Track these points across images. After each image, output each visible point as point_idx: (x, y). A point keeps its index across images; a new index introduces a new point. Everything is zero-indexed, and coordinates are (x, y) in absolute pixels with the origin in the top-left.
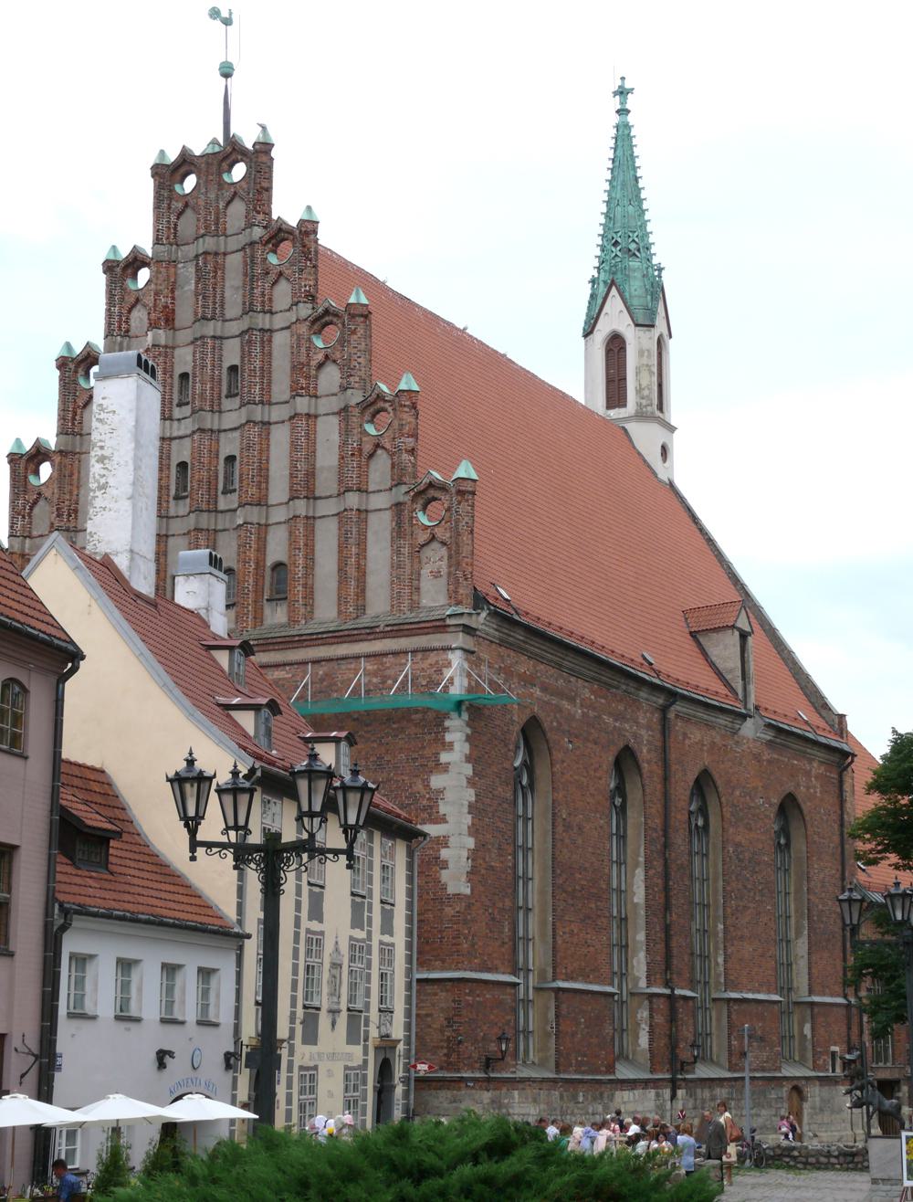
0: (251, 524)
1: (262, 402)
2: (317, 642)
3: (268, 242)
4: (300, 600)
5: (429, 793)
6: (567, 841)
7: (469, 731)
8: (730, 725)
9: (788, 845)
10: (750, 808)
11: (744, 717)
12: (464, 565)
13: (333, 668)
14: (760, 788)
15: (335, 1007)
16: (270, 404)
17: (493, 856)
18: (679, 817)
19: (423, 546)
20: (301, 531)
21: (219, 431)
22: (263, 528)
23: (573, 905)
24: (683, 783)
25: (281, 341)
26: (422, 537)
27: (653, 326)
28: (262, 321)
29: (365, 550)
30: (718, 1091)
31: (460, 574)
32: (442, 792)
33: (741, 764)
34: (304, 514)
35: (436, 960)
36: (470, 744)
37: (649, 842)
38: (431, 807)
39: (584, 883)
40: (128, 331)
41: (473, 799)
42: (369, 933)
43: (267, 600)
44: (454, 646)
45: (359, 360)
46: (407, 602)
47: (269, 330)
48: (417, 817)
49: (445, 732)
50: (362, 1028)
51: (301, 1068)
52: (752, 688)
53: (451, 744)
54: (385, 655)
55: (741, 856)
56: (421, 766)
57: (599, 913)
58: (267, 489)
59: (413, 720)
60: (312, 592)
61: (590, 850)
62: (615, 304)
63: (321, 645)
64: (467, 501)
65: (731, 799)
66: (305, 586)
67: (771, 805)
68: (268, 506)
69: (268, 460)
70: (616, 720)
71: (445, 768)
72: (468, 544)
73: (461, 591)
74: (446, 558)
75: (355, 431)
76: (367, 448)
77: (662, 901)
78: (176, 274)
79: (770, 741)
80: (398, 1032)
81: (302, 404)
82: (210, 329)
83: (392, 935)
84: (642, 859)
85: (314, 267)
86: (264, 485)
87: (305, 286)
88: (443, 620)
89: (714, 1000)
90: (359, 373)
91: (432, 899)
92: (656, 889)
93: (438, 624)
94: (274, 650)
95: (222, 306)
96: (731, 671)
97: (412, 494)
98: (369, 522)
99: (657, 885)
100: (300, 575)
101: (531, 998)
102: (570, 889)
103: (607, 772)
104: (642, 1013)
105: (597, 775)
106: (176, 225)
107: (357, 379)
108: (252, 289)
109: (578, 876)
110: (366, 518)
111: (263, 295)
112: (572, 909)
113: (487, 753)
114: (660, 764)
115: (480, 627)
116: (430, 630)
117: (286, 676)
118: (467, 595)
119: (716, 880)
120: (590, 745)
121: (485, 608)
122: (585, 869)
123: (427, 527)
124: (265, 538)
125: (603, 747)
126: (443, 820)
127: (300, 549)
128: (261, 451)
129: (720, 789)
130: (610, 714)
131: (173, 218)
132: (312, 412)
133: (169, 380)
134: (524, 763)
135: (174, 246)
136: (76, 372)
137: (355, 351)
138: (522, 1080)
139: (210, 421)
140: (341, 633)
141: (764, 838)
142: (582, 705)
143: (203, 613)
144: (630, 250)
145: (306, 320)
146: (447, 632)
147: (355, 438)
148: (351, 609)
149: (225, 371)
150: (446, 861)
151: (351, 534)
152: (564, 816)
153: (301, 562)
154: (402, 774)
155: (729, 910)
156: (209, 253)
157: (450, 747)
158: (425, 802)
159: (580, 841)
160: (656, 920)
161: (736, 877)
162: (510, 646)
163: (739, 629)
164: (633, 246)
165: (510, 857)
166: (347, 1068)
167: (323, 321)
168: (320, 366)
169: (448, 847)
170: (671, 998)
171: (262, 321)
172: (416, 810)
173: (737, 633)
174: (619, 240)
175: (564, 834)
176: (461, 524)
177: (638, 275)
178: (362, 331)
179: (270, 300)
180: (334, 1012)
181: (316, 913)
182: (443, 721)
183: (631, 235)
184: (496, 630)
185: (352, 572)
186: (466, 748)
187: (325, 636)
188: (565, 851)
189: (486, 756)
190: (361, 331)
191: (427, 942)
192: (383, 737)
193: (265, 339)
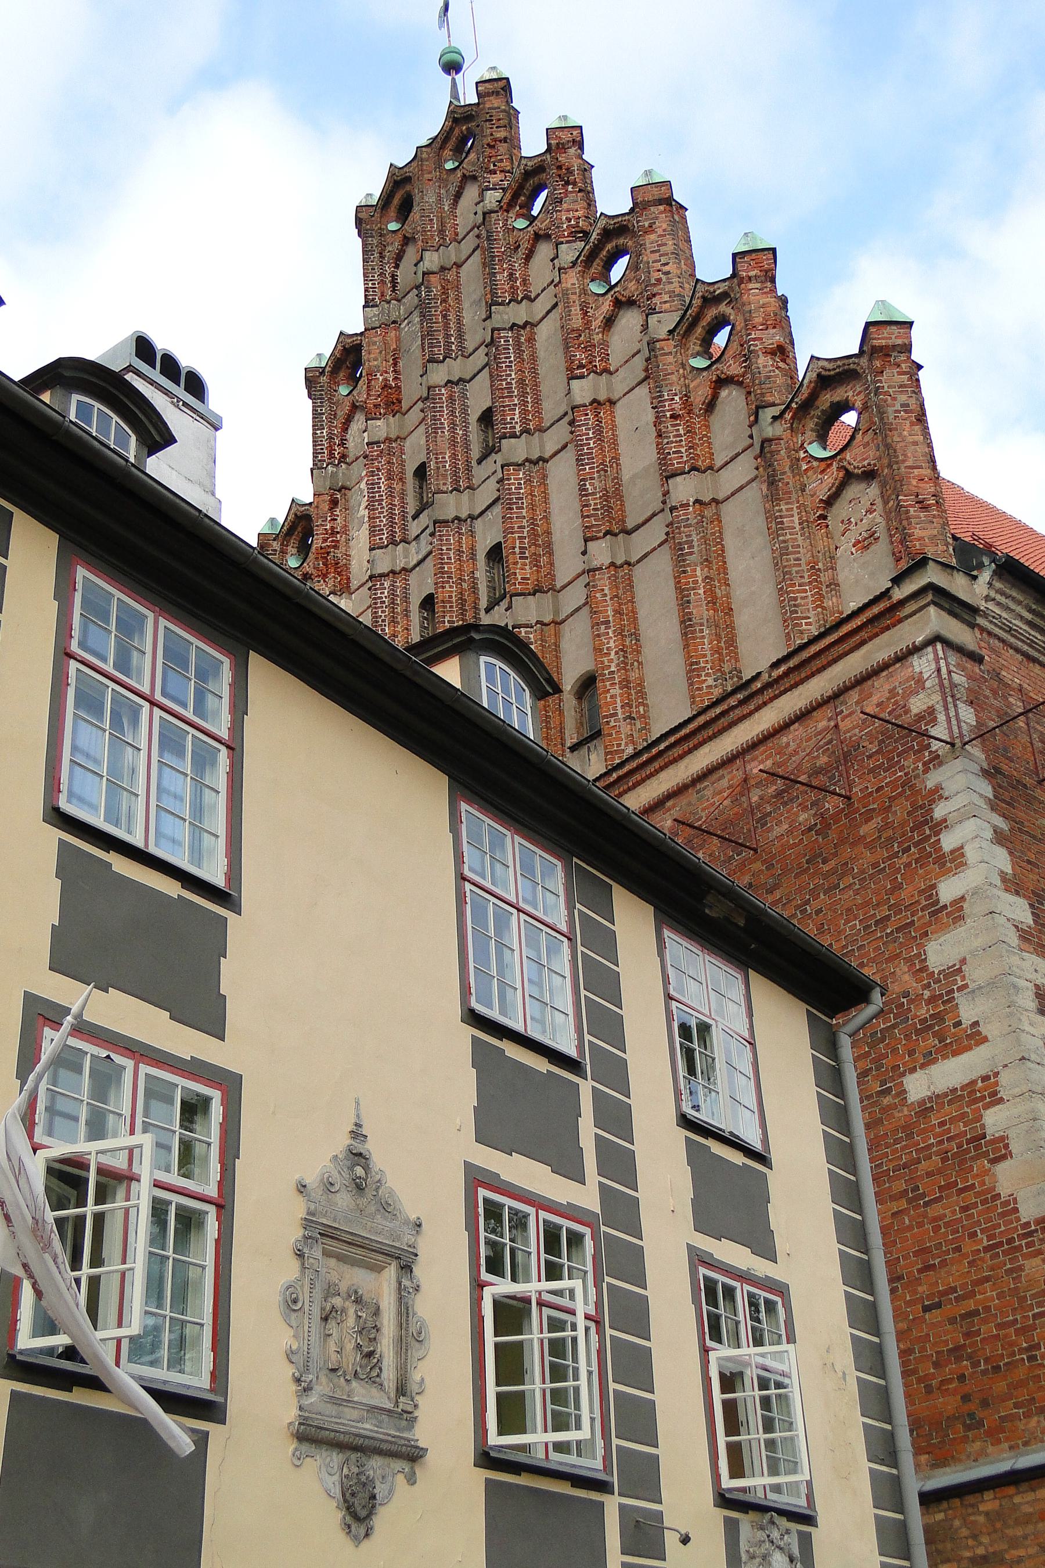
0: (526, 626)
1: (526, 431)
2: (649, 769)
4: (620, 712)
5: (928, 985)
12: (914, 482)
13: (689, 804)
16: (542, 430)
19: (829, 502)
20: (606, 591)
21: (473, 518)
25: (547, 333)
26: (821, 485)
28: (519, 313)
29: (724, 569)
32: (960, 970)
34: (607, 562)
35: (1028, 1415)
36: (1011, 853)
38: (939, 1017)
40: (343, 457)
44: (919, 640)
45: (666, 268)
46: (812, 614)
47: (527, 323)
48: (911, 1053)
49: (937, 834)
53: (958, 853)
56: (898, 930)
58: (552, 564)
59: (864, 837)
60: (642, 694)
63: (661, 769)
66: (625, 684)
69: (546, 518)
71: (956, 912)
72: (916, 443)
73: (918, 533)
74: (879, 501)
76: (701, 393)
78: (398, 339)
81: (583, 390)
85: (580, 191)
86: (544, 560)
87: (569, 220)
88: (885, 594)
91: (987, 1249)
93: (876, 610)
97: (788, 416)
106: (394, 277)
107: (666, 298)
115: (983, 605)
116: (864, 634)
121: (986, 561)
124: (557, 645)
126: (975, 1037)
128: (532, 507)
131: (388, 269)
132: (602, 397)
137: (656, 256)
139: (450, 505)
140: (692, 726)
145: (574, 264)
146: (900, 621)
147: (676, 388)
148: (710, 681)
149: (473, 426)
150: (1002, 1139)
151: (691, 547)
153: (612, 644)
157: (957, 860)
158: (924, 1011)
168: (609, 322)
169: (1001, 1100)
171: (519, 313)
172: (907, 1037)
176: (890, 410)
178: (664, 226)
179: (525, 282)
182: (931, 810)
184: (1030, 623)
185: (700, 611)
186: (1002, 860)
187: (662, 747)
190: (662, 224)
191: (997, 1369)
192: (807, 902)
193: (523, 339)
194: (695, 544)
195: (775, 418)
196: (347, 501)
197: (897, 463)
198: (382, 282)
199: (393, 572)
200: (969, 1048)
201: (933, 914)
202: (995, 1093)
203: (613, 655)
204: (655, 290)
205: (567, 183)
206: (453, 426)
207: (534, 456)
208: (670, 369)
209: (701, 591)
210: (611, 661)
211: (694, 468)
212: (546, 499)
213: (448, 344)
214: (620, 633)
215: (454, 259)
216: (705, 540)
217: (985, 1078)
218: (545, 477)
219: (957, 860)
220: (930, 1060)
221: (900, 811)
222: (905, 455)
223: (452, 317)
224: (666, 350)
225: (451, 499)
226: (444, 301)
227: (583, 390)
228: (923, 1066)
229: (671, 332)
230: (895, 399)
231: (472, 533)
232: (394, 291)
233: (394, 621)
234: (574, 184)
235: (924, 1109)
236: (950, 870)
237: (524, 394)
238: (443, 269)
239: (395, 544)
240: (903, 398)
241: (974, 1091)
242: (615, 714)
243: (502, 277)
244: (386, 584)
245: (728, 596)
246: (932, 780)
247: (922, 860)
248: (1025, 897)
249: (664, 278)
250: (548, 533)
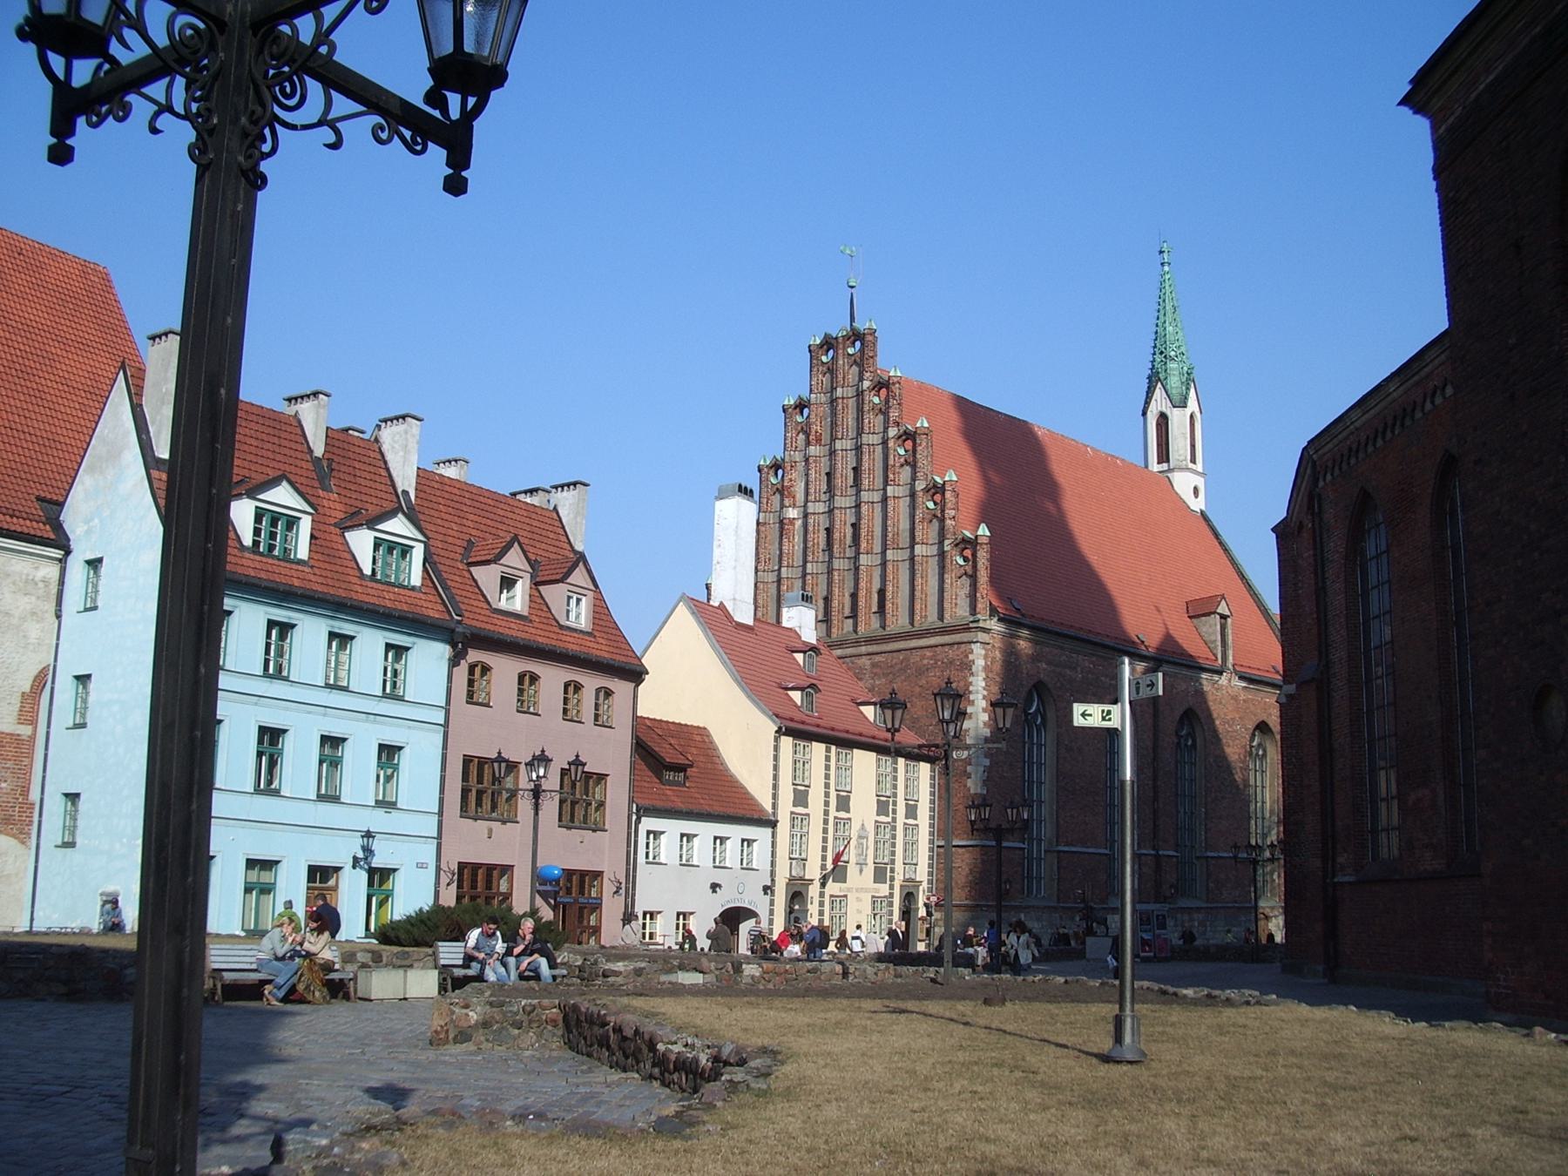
7: (985, 693)
9: (1265, 755)
11: (1220, 673)
15: (862, 862)
30: (1195, 916)
33: (1221, 703)
41: (989, 735)
42: (894, 820)
50: (888, 874)
51: (831, 896)
52: (1230, 653)
54: (936, 646)
62: (1159, 392)
80: (922, 874)
83: (916, 819)
89: (1198, 858)
111: (870, 423)
114: (1151, 706)
123: (961, 566)
129: (1203, 720)
130: (1107, 676)
134: (1038, 709)
138: (1029, 907)
142: (1082, 672)
143: (797, 629)
155: (1209, 799)
164: (1173, 353)
166: (873, 897)
170: (1157, 857)
173: (1218, 617)
177: (1176, 373)
180: (861, 865)
181: (844, 804)
219: (972, 703)
221: (962, 684)
246: (971, 679)
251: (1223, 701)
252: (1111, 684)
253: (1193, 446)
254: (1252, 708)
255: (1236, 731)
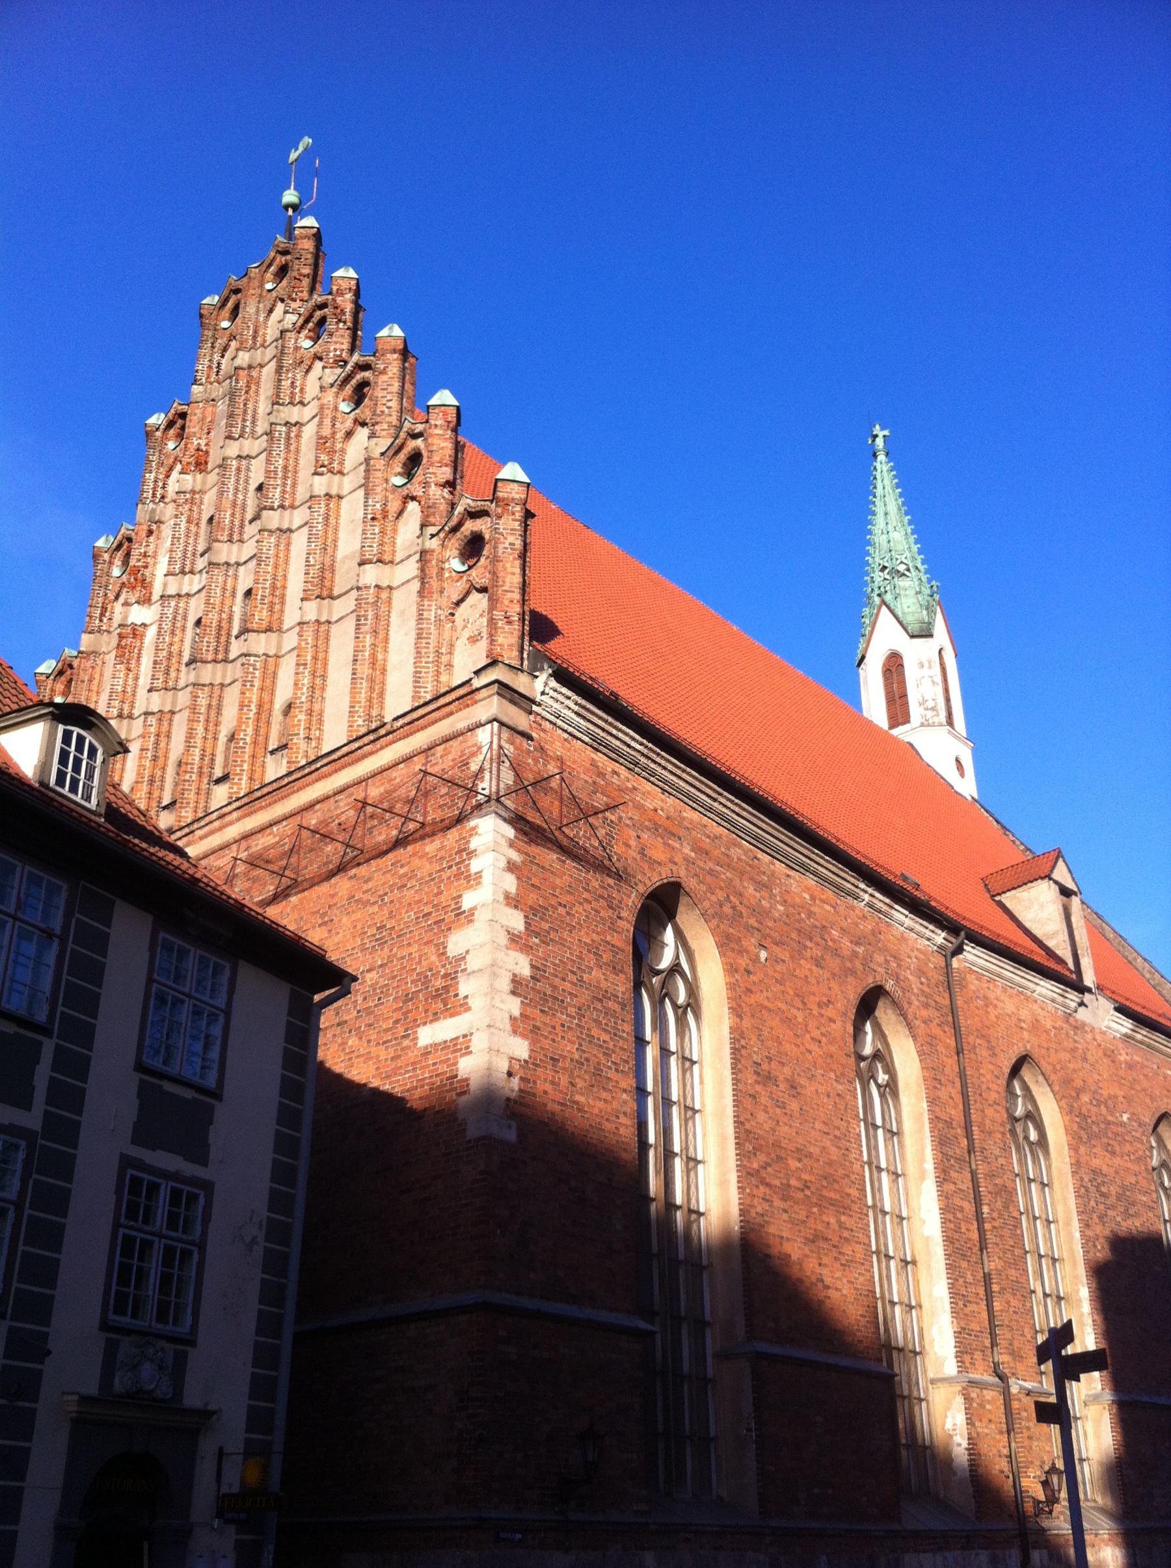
0: (256, 656)
1: (282, 507)
3: (302, 327)
4: (302, 732)
5: (444, 966)
6: (764, 1100)
8: (1060, 999)
10: (1109, 1123)
12: (506, 602)
13: (329, 810)
14: (1121, 1099)
17: (580, 1084)
18: (990, 1112)
21: (238, 564)
22: (271, 661)
23: (785, 1211)
24: (991, 1067)
25: (309, 431)
27: (931, 636)
28: (294, 414)
31: (499, 615)
32: (464, 958)
33: (1085, 1059)
34: (313, 620)
36: (518, 878)
37: (942, 1142)
38: (446, 989)
39: (806, 1177)
41: (526, 971)
43: (272, 753)
47: (297, 423)
48: (426, 1011)
49: (470, 859)
55: (1103, 1189)
56: (435, 923)
57: (846, 1234)
59: (428, 853)
61: (818, 1125)
63: (317, 781)
64: (513, 514)
65: (1075, 1105)
66: (310, 713)
67: (1140, 1125)
68: (280, 630)
69: (285, 576)
70: (857, 944)
75: (379, 489)
76: (393, 507)
77: (975, 1236)
79: (1126, 1035)
81: (320, 485)
82: (233, 449)
84: (929, 1166)
86: (277, 607)
87: (335, 350)
88: (469, 681)
90: (388, 419)
92: (959, 1215)
94: (261, 808)
95: (254, 422)
96: (1052, 936)
97: (442, 535)
98: (395, 603)
99: (962, 1209)
100: (303, 699)
101: (710, 1373)
102: (777, 1183)
103: (845, 1014)
104: (954, 1417)
105: (829, 1012)
108: (280, 381)
109: (793, 1164)
110: (390, 598)
112: (785, 1216)
113: (560, 904)
115: (538, 698)
117: (273, 841)
118: (510, 645)
119: (1068, 1223)
120: (802, 962)
121: (546, 667)
122: (810, 1155)
125: (834, 975)
126: (465, 1007)
127: (306, 664)
128: (276, 567)
131: (216, 357)
132: (334, 492)
133: (193, 528)
135: (216, 384)
136: (111, 563)
139: (225, 552)
140: (339, 753)
141: (1136, 1168)
144: (899, 572)
145: (332, 385)
147: (378, 498)
151: (366, 619)
152: (755, 1057)
153: (306, 681)
154: (409, 945)
156: (243, 369)
159: (794, 1106)
160: (964, 1264)
161: (1101, 1217)
162: (615, 755)
163: (1056, 882)
164: (902, 568)
165: (624, 1096)
167: (354, 382)
168: (349, 434)
171: (294, 414)
172: (426, 1000)
174: (886, 564)
175: (758, 1088)
176: (501, 546)
179: (302, 390)
182: (468, 842)
183: (898, 557)
185: (364, 670)
187: (318, 765)
188: (761, 1116)
189: (561, 910)
192: (386, 894)
193: (292, 435)
194: (370, 617)
195: (433, 536)
196: (160, 532)
197: (497, 586)
198: (210, 367)
199: (179, 595)
200: (459, 1013)
201: (457, 915)
202: (467, 1048)
203: (305, 690)
204: (378, 419)
205: (340, 321)
206: (236, 489)
207: (285, 527)
208: (377, 481)
209: (367, 654)
210: (303, 694)
211: (379, 561)
212: (287, 561)
213: (244, 427)
214: (313, 674)
215: (259, 361)
216: (377, 617)
217: (465, 1036)
218: (288, 544)
220: (436, 1017)
222: (504, 582)
223: (250, 405)
224: (378, 467)
225: (225, 547)
226: (247, 392)
227: (320, 485)
228: (431, 1022)
229: (383, 454)
230: (506, 539)
231: (236, 577)
232: (217, 375)
233: (173, 633)
234: (345, 322)
235: (426, 1053)
236: (472, 886)
237: (285, 478)
238: (250, 367)
239: (183, 572)
240: (511, 539)
241: (455, 1045)
242: (298, 734)
243: (286, 384)
244: (173, 604)
245: (385, 660)
247: (458, 876)
248: (522, 910)
249: (387, 411)
250: (284, 587)
251: (1089, 1056)
252: (855, 954)
253: (948, 700)
254: (1145, 1084)
255: (1122, 1124)
